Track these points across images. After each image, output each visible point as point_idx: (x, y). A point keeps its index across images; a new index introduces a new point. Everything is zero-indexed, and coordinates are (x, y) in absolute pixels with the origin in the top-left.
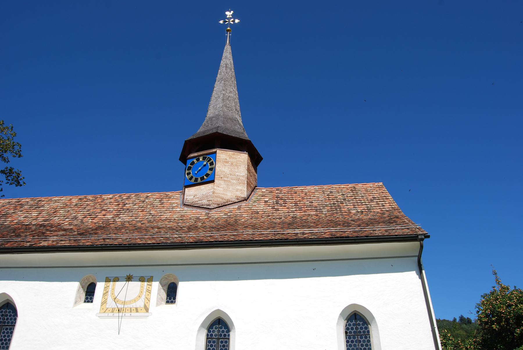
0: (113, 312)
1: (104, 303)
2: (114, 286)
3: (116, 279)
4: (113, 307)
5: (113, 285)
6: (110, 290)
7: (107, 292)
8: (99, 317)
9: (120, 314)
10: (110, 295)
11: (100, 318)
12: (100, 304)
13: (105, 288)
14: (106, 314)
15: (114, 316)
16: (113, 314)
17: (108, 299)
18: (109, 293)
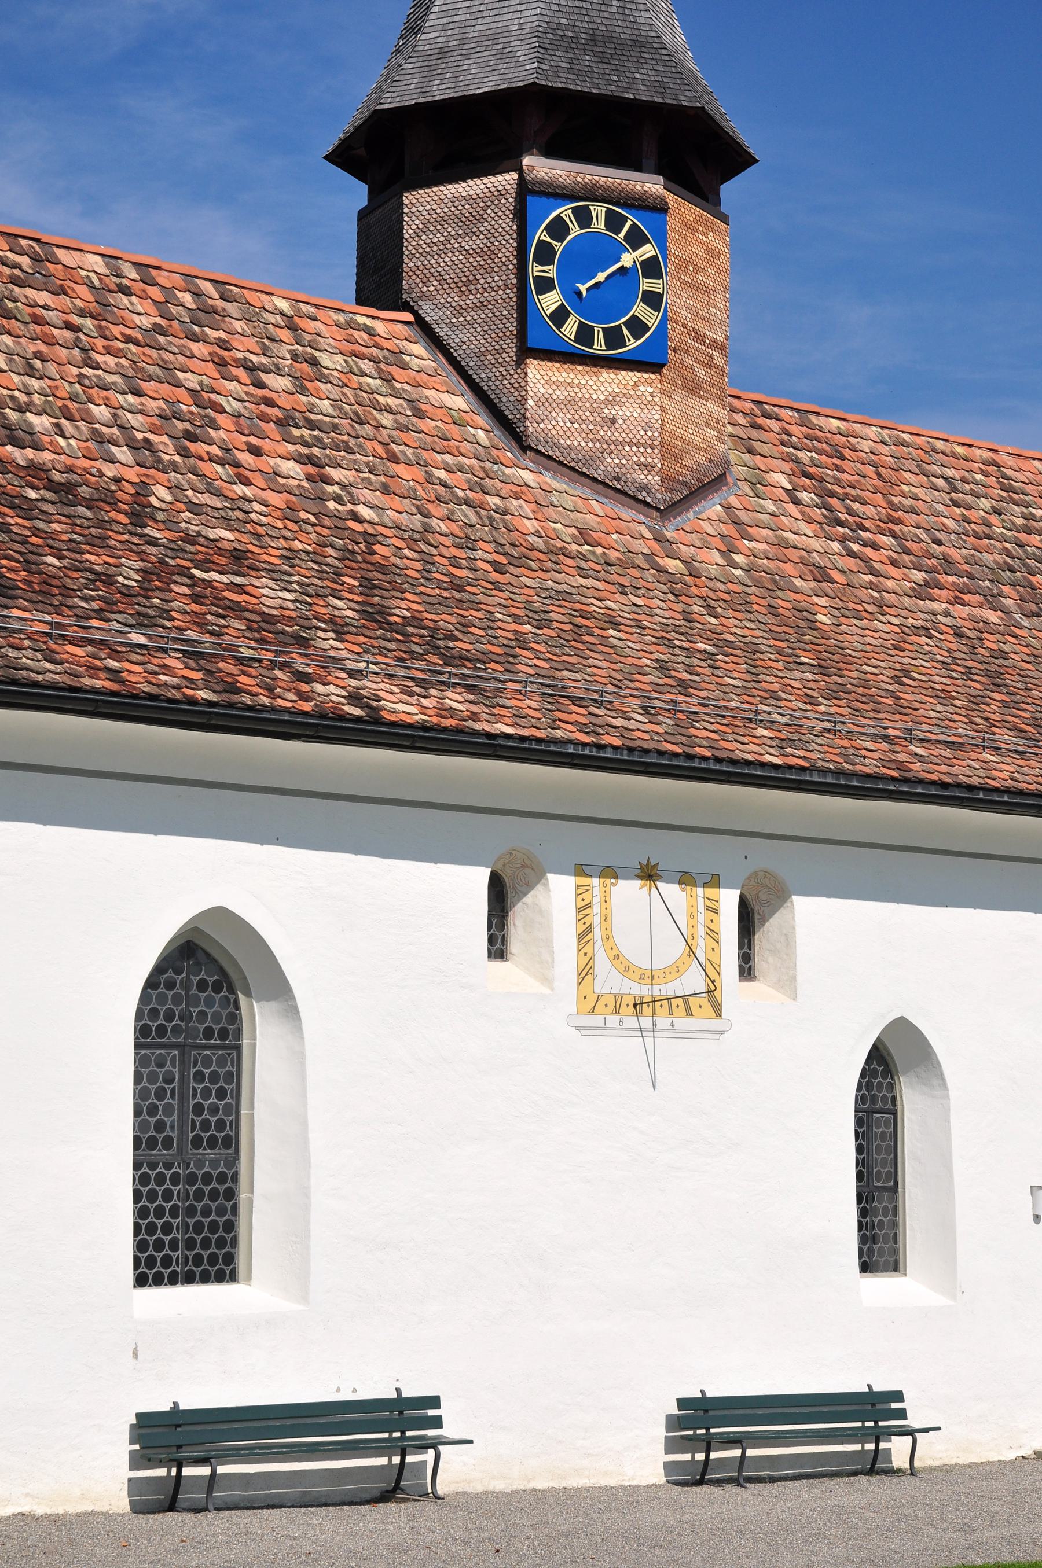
0: (617, 1012)
1: (585, 973)
2: (607, 905)
3: (610, 873)
4: (615, 991)
5: (603, 899)
6: (597, 920)
7: (589, 930)
8: (578, 1029)
9: (646, 1022)
10: (600, 941)
11: (583, 1032)
12: (574, 979)
13: (580, 910)
14: (597, 1020)
15: (622, 1029)
16: (617, 1018)
17: (596, 958)
18: (597, 932)
